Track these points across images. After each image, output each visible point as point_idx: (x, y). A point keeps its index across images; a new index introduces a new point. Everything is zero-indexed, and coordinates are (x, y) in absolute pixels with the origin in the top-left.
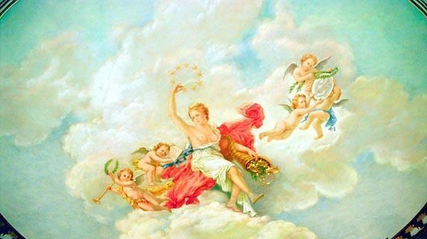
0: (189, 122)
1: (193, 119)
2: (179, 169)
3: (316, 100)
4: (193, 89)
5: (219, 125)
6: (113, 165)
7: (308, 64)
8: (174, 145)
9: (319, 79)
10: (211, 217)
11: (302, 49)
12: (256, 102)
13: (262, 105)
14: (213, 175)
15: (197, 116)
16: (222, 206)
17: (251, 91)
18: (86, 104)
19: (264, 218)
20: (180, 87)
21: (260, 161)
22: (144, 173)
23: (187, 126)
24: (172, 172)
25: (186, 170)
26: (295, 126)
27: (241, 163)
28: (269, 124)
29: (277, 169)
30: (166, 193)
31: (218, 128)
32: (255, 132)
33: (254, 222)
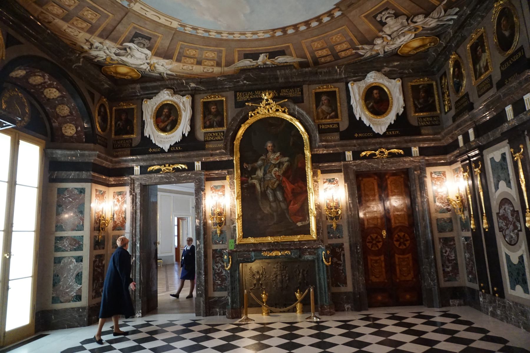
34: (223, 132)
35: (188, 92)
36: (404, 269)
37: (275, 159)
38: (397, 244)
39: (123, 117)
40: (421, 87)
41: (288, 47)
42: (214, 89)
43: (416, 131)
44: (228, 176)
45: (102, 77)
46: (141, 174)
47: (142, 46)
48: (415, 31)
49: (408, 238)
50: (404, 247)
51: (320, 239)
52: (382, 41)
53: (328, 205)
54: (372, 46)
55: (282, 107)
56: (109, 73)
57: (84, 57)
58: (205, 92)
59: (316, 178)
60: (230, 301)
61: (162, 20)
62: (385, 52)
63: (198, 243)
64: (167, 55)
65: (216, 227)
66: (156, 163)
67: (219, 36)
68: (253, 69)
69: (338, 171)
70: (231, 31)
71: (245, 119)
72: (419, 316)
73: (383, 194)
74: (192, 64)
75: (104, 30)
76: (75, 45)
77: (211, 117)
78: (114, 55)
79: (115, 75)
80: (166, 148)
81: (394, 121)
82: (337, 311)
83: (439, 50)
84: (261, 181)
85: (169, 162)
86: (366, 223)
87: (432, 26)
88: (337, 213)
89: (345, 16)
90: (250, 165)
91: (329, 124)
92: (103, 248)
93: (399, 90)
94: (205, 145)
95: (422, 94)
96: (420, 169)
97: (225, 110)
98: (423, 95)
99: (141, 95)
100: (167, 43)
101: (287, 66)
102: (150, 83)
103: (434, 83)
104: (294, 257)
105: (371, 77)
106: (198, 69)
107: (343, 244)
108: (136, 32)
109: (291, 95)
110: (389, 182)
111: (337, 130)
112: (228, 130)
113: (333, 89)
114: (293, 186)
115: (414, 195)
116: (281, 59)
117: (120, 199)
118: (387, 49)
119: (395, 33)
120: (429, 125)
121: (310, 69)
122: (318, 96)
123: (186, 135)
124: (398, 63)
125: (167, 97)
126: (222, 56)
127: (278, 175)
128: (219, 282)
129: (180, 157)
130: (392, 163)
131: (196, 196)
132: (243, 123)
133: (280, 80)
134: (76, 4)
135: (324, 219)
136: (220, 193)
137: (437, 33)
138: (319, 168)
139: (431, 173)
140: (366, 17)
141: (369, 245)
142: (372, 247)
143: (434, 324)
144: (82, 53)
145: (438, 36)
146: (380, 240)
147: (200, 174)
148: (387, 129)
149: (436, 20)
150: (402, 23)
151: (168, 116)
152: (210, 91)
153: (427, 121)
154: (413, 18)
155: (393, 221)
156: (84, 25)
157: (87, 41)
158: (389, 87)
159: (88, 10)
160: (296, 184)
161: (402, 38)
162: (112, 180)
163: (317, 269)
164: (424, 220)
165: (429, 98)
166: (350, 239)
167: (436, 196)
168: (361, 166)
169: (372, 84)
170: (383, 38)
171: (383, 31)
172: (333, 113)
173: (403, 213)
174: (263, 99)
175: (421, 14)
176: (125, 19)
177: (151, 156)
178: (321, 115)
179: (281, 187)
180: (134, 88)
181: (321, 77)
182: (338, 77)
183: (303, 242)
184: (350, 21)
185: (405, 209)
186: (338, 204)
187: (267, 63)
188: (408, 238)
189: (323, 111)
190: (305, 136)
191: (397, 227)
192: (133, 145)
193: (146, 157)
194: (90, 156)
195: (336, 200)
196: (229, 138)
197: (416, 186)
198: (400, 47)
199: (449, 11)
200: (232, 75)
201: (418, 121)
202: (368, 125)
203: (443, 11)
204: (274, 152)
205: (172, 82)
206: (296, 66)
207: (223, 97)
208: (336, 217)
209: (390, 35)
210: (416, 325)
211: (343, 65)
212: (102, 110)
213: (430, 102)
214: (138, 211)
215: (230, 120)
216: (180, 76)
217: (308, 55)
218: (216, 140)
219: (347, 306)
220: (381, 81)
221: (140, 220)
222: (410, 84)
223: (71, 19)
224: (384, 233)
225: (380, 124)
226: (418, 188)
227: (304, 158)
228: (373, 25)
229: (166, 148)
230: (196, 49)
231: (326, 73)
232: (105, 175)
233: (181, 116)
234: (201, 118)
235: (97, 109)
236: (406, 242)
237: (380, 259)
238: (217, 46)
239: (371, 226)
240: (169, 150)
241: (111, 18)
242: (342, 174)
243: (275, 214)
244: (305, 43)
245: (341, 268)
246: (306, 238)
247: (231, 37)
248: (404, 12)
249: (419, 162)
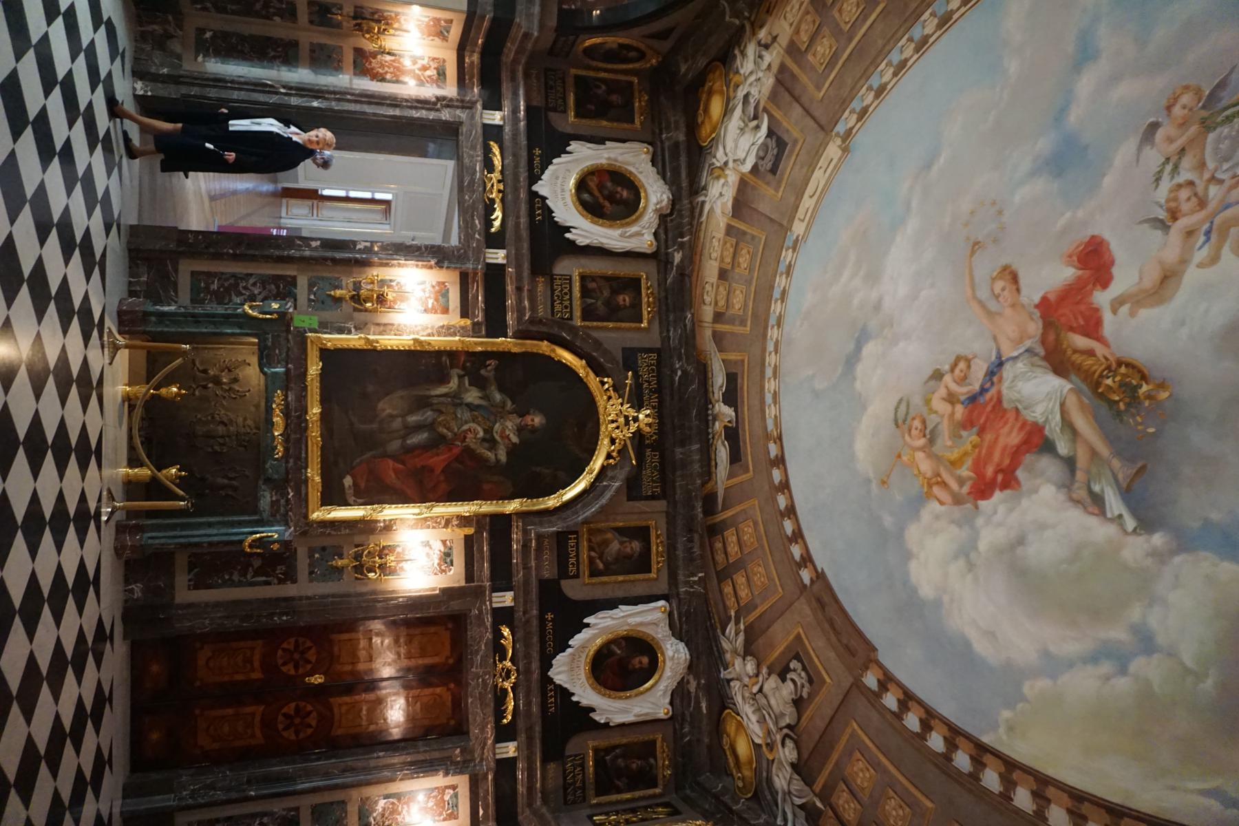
0: (993, 306)
1: (997, 297)
2: (986, 404)
3: (1221, 182)
4: (994, 241)
5: (1037, 299)
6: (903, 408)
7: (1184, 107)
8: (975, 357)
9: (1219, 130)
10: (1042, 527)
11: (1161, 83)
12: (1096, 233)
13: (1107, 235)
14: (1037, 414)
15: (1003, 289)
16: (1062, 496)
17: (1080, 214)
18: (878, 307)
19: (1158, 539)
20: (976, 243)
21: (1123, 370)
22: (938, 420)
23: (990, 314)
24: (975, 414)
25: (994, 407)
26: (1184, 261)
27: (1085, 380)
28: (1124, 279)
29: (1162, 386)
30: (969, 462)
31: (1037, 306)
32: (1102, 298)
33: (1136, 549)
34: (571, 318)
35: (663, 247)
36: (226, 729)
37: (503, 431)
38: (290, 708)
39: (615, 98)
40: (652, 761)
41: (747, 471)
42: (667, 305)
43: (553, 751)
44: (469, 322)
45: (702, 62)
46: (485, 126)
47: (761, 154)
48: (767, 745)
49: (302, 736)
50: (281, 727)
51: (308, 528)
53: (391, 549)
55: (619, 452)
56: (711, 76)
57: (743, 27)
58: (662, 283)
59: (455, 522)
60: (166, 309)
61: (807, 203)
62: (729, 681)
63: (314, 244)
64: (741, 206)
65: (351, 286)
66: (506, 162)
67: (772, 321)
68: (706, 391)
69: (469, 576)
70: (782, 348)
71: (599, 370)
72: (101, 763)
73: (419, 679)
74: (722, 260)
75: (793, 76)
76: (768, 12)
77: (606, 293)
78: (745, 92)
79: (706, 88)
80: (541, 188)
81: (578, 703)
82: (127, 563)
83: (726, 799)
84: (454, 397)
85: (508, 190)
86: (346, 636)
87: (776, 779)
88: (370, 571)
89: (802, 593)
90: (492, 374)
91: (577, 556)
92: (311, 22)
93: (647, 714)
94: (543, 275)
96: (464, 762)
97: (619, 324)
98: (634, 766)
99: (662, 142)
100: (764, 207)
101: (709, 465)
102: (687, 163)
103: (658, 791)
104: (267, 466)
105: (677, 651)
106: (710, 271)
107: (294, 581)
108: (786, 144)
109: (647, 472)
110: (438, 690)
111: (563, 573)
112: (573, 330)
113: (654, 567)
114: (438, 471)
115: (404, 748)
116: (722, 453)
117: (428, 73)
118: (735, 685)
119: (764, 701)
120: (565, 779)
121: (701, 515)
122: (642, 533)
123: (567, 235)
125: (653, 199)
126: (733, 324)
127: (465, 438)
128: (215, 286)
129: (518, 217)
130: (482, 697)
131: (426, 247)
132: (589, 364)
133: (678, 450)
134: (842, 25)
135: (358, 539)
136: (431, 302)
137: (762, 795)
138: (479, 531)
139: (454, 787)
140: (798, 637)
141: (289, 644)
142: (284, 650)
143: (78, 798)
144: (752, 24)
145: (756, 797)
146: (301, 671)
147: (477, 260)
148: (560, 686)
149: (786, 787)
150: (783, 715)
151: (611, 198)
152: (663, 294)
153: (574, 777)
154: (791, 738)
155: (347, 699)
156: (805, 37)
157: (775, 38)
159: (831, 47)
160: (442, 478)
161: (754, 718)
162: (473, 58)
163: (236, 518)
164: (344, 771)
166: (308, 598)
167: (399, 800)
168: (479, 626)
169: (663, 654)
170: (757, 675)
171: (769, 675)
172: (601, 566)
173: (364, 723)
174: (638, 411)
175: (799, 754)
176: (812, 123)
177: (524, 154)
178: (597, 539)
179: (438, 442)
180: (677, 128)
181: (681, 540)
182: (681, 578)
183: (303, 488)
184: (791, 604)
185: (372, 727)
186: (393, 572)
187: (717, 424)
188: (302, 736)
189: (606, 543)
190: (552, 502)
191: (331, 710)
192: (552, 115)
193: (523, 141)
194: (529, 16)
195: (402, 568)
196: (555, 330)
197: (425, 751)
199: (802, 814)
200: (694, 346)
202: (570, 643)
203: (804, 801)
204: (520, 430)
205: (686, 213)
206: (709, 485)
207: (649, 323)
208: (362, 566)
209: (761, 690)
210: (78, 752)
211: (705, 588)
212: (633, 54)
213: (617, 782)
214: (397, 112)
215: (595, 334)
216: (698, 231)
217: (728, 514)
218: (553, 301)
219: (137, 589)
220: (668, 673)
221: (374, 114)
222: (659, 737)
223: (817, 11)
224: (318, 679)
225: (572, 669)
226: (421, 757)
227: (503, 498)
228: (783, 653)
229: (541, 188)
230: (751, 270)
231: (689, 550)
232: (484, 44)
233: (611, 226)
234: (604, 271)
235: (634, 43)
236: (292, 730)
237: (253, 670)
238: (755, 315)
239: (336, 649)
240: (536, 194)
241: (816, 94)
242: (463, 583)
243: (375, 426)
244: (753, 505)
245: (236, 577)
246: (314, 495)
247: (770, 347)
248: (804, 718)
249: (482, 760)
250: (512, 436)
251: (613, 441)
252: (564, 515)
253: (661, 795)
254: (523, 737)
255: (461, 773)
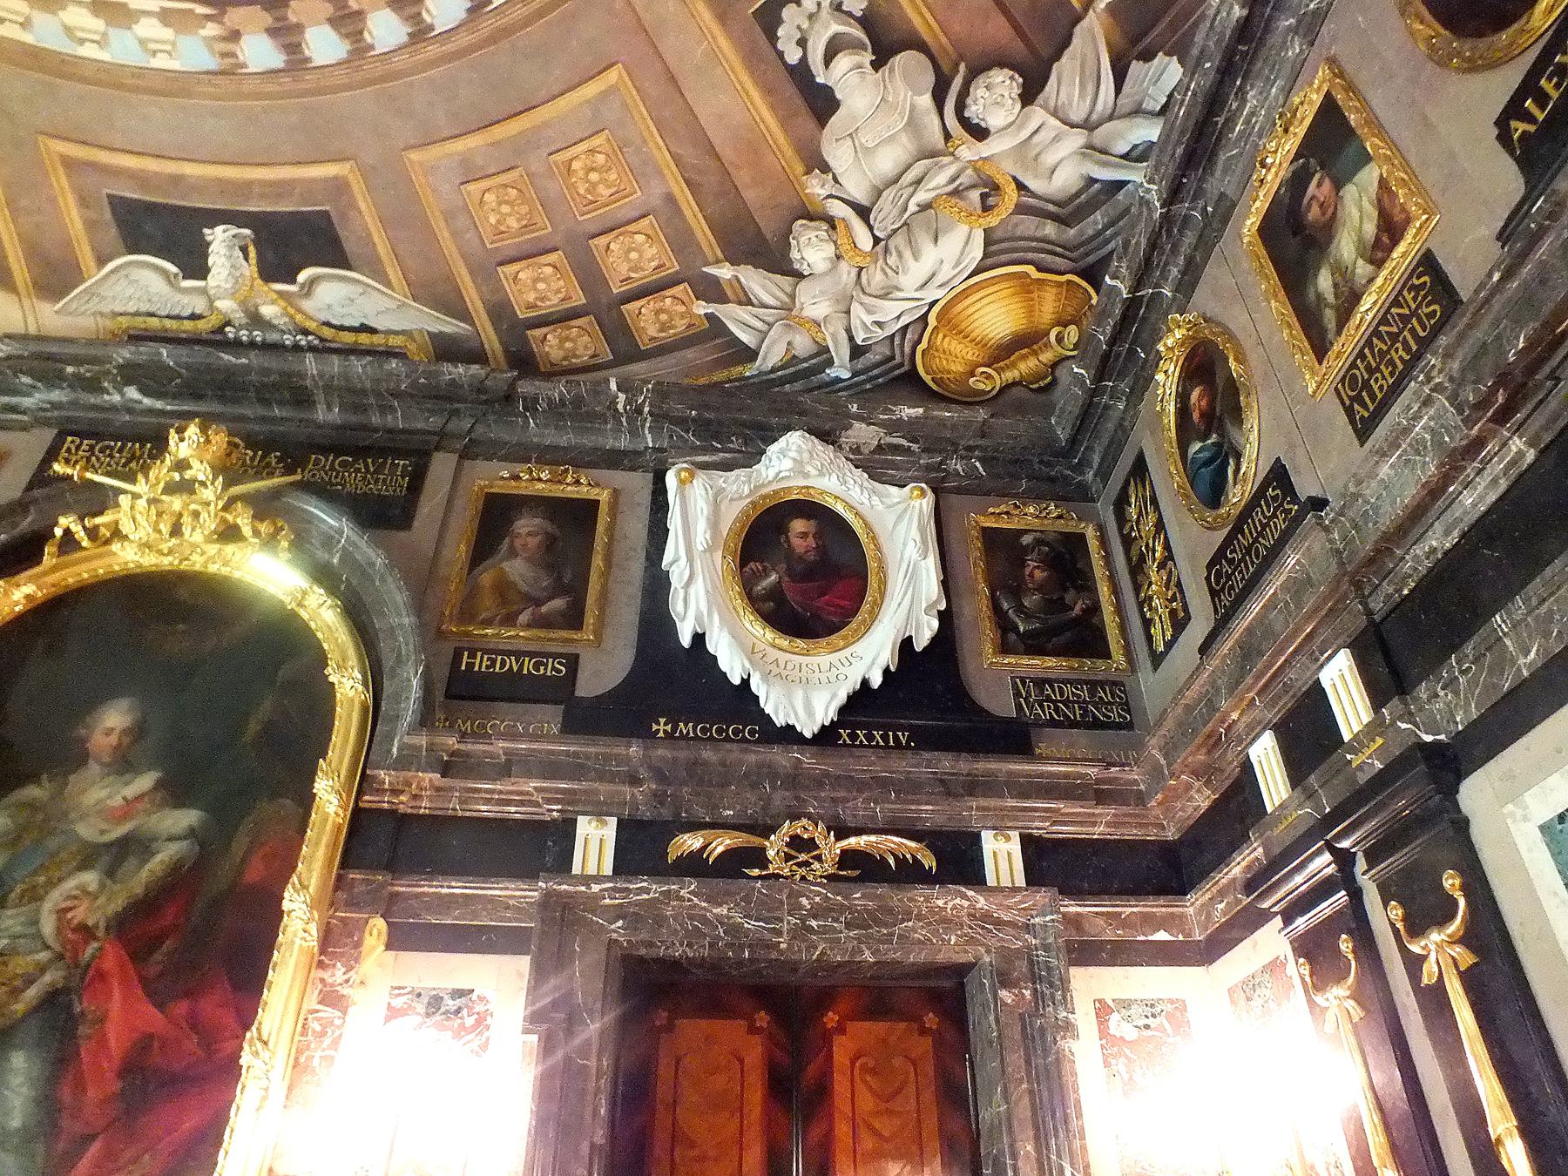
41: (339, 187)
52: (830, 250)
54: (785, 282)
59: (338, 974)
62: (857, 351)
81: (886, 672)
91: (518, 654)
95: (1035, 571)
96: (1034, 978)
98: (1038, 574)
103: (1090, 533)
105: (783, 453)
110: (840, 1057)
111: (559, 691)
114: (151, 1017)
120: (1074, 724)
122: (497, 515)
124: (921, 410)
138: (389, 907)
139: (1103, 1010)
148: (842, 711)
158: (864, 510)
160: (181, 1008)
165: (1069, 596)
168: (660, 921)
172: (558, 603)
181: (535, 430)
182: (623, 443)
189: (503, 588)
198: (924, 319)
201: (1017, 694)
202: (736, 680)
213: (1077, 610)
226: (1023, 1110)
249: (1027, 928)
250: (131, 791)
251: (229, 534)
252: (388, 663)
253: (1101, 528)
254: (970, 811)
255: (1064, 984)
